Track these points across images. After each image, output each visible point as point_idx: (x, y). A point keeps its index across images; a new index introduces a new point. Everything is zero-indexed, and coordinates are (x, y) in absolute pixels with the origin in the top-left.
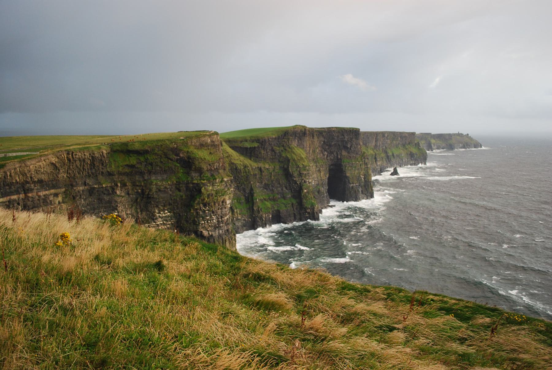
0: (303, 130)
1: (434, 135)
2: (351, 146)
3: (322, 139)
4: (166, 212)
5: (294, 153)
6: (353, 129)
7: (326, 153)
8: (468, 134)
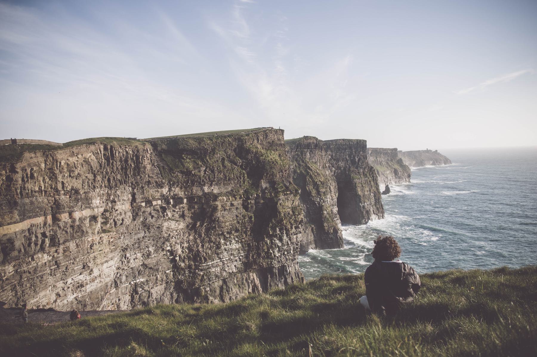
0: (315, 141)
1: (404, 153)
2: (359, 160)
3: (329, 152)
4: (233, 241)
5: (309, 168)
6: (360, 141)
7: (333, 169)
8: (436, 151)
